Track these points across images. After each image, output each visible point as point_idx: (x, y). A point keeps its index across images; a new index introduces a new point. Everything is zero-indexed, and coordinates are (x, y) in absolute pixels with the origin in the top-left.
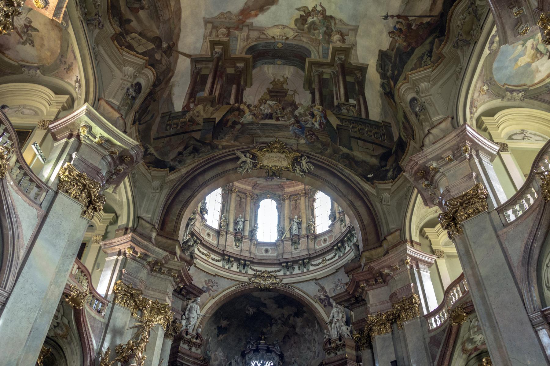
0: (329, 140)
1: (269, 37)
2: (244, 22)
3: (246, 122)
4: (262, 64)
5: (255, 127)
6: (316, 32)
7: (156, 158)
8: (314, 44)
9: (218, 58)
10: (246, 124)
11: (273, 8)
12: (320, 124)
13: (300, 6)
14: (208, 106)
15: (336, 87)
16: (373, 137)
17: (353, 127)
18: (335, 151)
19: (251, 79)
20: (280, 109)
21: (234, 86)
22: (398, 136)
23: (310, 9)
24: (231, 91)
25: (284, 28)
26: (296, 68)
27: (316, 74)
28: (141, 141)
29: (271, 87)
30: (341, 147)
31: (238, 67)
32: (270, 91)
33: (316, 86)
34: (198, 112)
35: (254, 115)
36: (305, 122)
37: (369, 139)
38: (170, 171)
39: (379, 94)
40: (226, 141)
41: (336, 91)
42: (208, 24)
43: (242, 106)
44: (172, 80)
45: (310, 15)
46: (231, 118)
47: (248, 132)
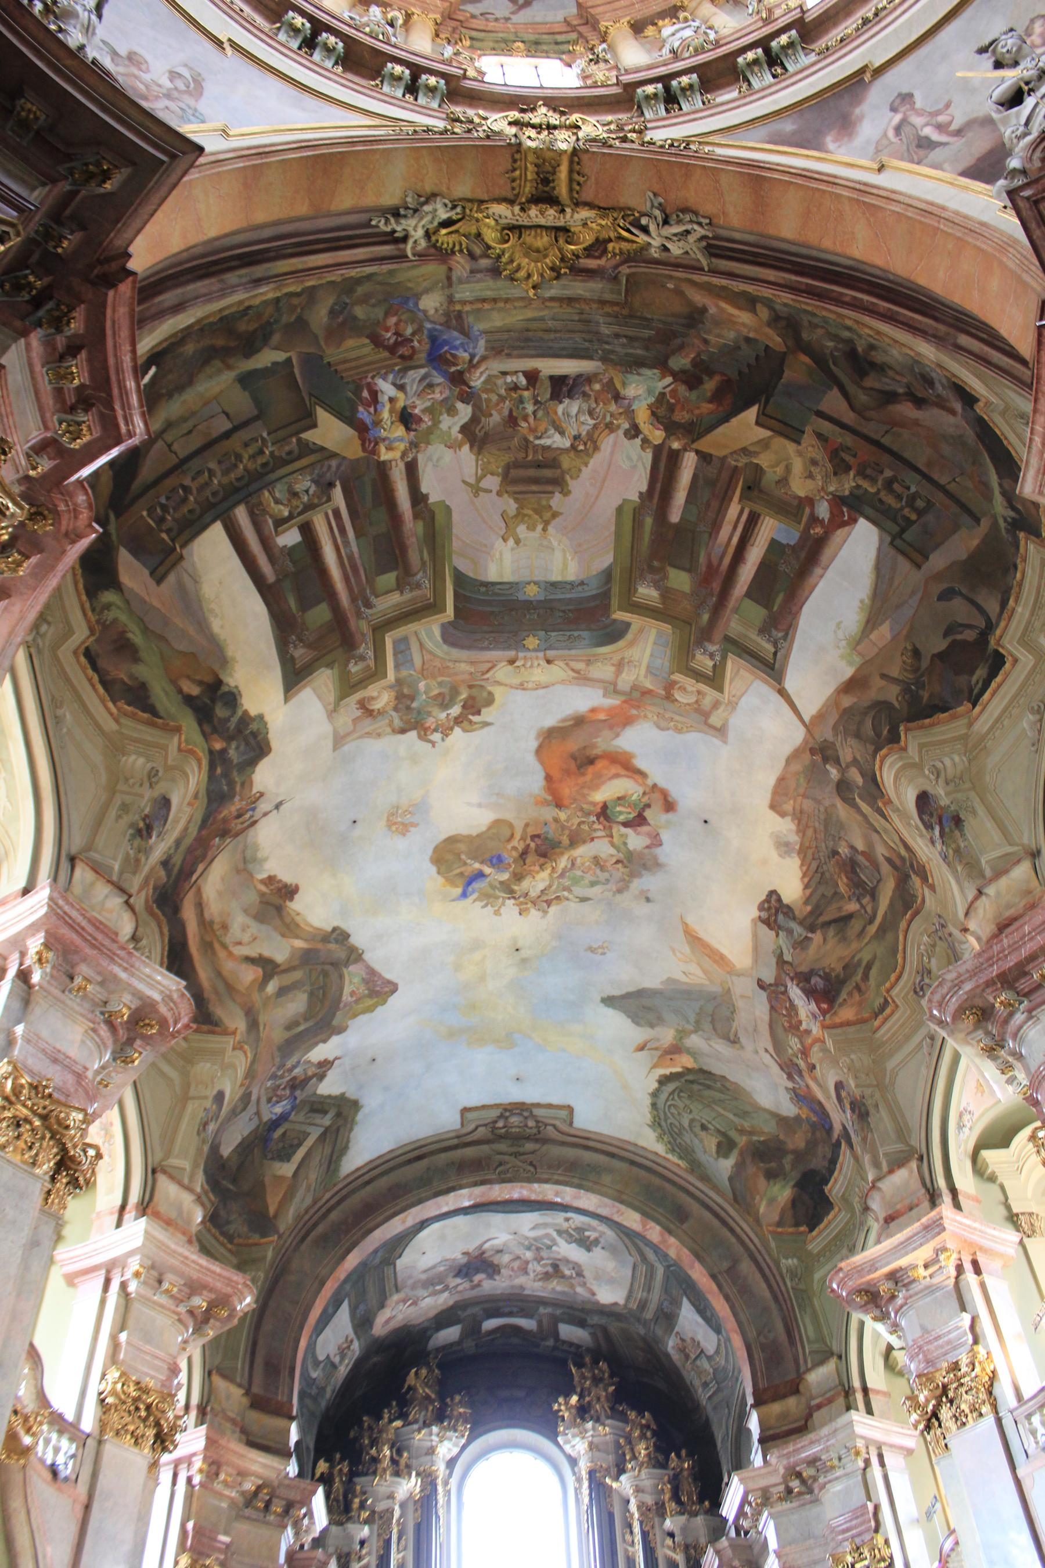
0: (333, 354)
1: (561, 664)
2: (624, 702)
3: (648, 372)
4: (582, 583)
5: (619, 347)
6: (436, 692)
7: (1000, 477)
8: (437, 663)
9: (710, 640)
10: (651, 367)
11: (550, 722)
12: (374, 394)
13: (486, 730)
14: (772, 474)
15: (351, 558)
16: (187, 482)
17: (261, 452)
18: (300, 326)
19: (618, 534)
20: (525, 418)
21: (675, 516)
22: (125, 578)
23: (457, 730)
24: (688, 501)
25: (522, 684)
26: (483, 579)
27: (418, 577)
28: (1015, 567)
29: (557, 500)
30: (280, 356)
31: (656, 585)
32: (559, 483)
33: (412, 527)
34: (811, 476)
35: (617, 397)
36: (431, 386)
37: (195, 464)
38: (977, 400)
39: (230, 652)
40: (737, 324)
41: (347, 543)
42: (718, 726)
43: (657, 436)
44: (849, 672)
45: (456, 718)
46: (699, 404)
47: (647, 333)
